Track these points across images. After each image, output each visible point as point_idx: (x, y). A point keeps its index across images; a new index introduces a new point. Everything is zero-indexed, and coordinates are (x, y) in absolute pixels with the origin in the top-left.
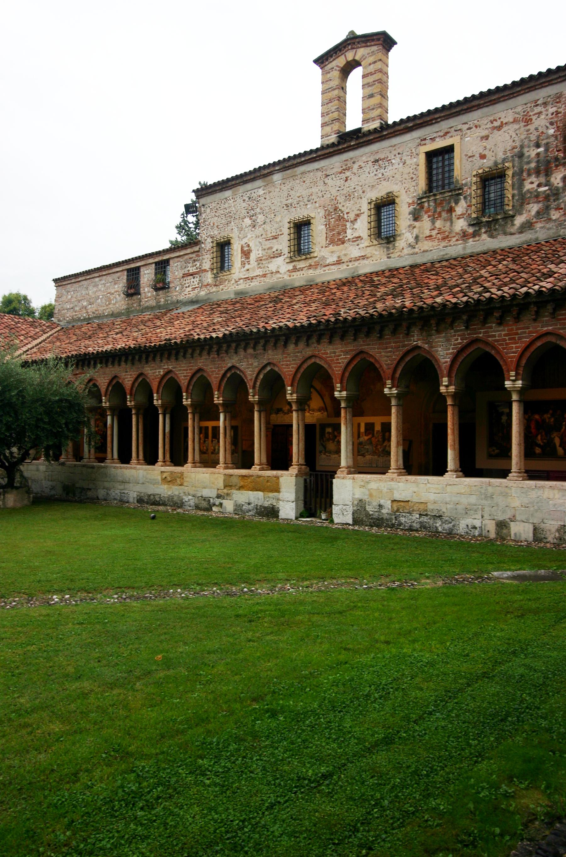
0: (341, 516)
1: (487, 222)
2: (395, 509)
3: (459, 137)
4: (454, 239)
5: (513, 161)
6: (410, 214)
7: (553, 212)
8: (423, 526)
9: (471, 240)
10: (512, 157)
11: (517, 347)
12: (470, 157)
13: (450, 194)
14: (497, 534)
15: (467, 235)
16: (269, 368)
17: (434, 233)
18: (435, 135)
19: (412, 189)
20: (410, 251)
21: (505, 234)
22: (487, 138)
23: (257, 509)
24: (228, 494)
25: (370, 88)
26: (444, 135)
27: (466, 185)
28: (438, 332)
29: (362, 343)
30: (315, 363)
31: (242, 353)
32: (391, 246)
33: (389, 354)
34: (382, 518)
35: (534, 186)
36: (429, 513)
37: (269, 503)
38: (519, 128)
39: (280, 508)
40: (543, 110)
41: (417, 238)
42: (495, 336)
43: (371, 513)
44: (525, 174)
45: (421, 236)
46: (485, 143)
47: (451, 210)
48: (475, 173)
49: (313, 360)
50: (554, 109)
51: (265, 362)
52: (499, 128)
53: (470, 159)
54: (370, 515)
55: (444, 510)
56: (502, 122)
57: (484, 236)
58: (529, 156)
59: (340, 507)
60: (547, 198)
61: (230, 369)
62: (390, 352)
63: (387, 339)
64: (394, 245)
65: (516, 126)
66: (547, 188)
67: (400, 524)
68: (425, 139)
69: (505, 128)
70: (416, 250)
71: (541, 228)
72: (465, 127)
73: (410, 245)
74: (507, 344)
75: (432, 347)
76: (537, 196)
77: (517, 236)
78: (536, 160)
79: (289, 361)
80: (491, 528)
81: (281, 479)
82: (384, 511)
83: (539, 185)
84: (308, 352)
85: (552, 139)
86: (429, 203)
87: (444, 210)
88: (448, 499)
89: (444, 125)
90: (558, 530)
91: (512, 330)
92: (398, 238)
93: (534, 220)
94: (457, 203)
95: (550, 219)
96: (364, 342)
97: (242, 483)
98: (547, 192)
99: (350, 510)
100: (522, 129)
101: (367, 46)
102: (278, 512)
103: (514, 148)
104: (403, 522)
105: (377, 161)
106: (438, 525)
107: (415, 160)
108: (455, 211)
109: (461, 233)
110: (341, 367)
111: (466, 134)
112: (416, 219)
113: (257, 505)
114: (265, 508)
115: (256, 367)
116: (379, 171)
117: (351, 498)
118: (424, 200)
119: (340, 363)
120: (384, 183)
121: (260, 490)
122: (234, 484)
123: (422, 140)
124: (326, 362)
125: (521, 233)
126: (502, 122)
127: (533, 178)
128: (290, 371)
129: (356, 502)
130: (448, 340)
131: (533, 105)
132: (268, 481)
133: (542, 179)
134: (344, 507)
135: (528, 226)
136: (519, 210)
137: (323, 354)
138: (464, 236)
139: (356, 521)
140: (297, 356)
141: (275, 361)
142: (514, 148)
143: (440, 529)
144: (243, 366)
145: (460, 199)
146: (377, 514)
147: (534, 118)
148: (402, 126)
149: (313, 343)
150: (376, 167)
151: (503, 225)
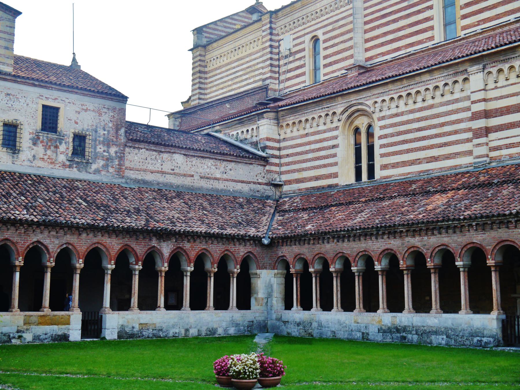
0: (111, 335)
1: (77, 161)
2: (141, 328)
3: (64, 105)
4: (58, 165)
5: (92, 133)
6: (30, 139)
7: (110, 168)
8: (154, 335)
9: (68, 169)
10: (92, 130)
11: (194, 253)
12: (69, 120)
13: (57, 137)
14: (185, 334)
15: (65, 166)
16: (65, 246)
17: (46, 157)
18: (49, 96)
19: (32, 124)
20: (29, 163)
21: (86, 171)
22: (79, 113)
23: (52, 337)
24: (27, 330)
25: (6, 43)
26: (54, 99)
27: (66, 135)
28: (164, 241)
29: (127, 240)
30: (97, 247)
31: (46, 233)
32: (15, 156)
33: (141, 248)
34: (134, 334)
35: (102, 150)
36: (157, 328)
37: (62, 332)
38: (96, 116)
39: (70, 335)
40: (107, 112)
41: (34, 156)
42: (186, 247)
43: (128, 331)
44: (97, 142)
45: (37, 156)
46: (77, 115)
47: (56, 147)
48: (73, 131)
49: (96, 245)
50: (112, 114)
51: (64, 242)
52: (86, 110)
53: (69, 121)
54: (127, 333)
55: (164, 326)
56: (87, 108)
57: (75, 169)
58: (100, 133)
59: (110, 330)
60: (107, 159)
61: (33, 243)
62: (141, 247)
63: (140, 240)
64: (18, 156)
65: (93, 114)
66: (107, 154)
67: (143, 336)
68: (42, 96)
69: (88, 112)
70: (33, 164)
71: (104, 175)
72: (67, 101)
73: (29, 160)
74: (190, 251)
75: (161, 248)
76: (103, 157)
77: (92, 175)
78: (103, 137)
79: (82, 244)
80: (183, 332)
81: (71, 316)
82: (135, 330)
83: (104, 151)
84: (95, 240)
85: (111, 129)
86: (43, 138)
87: (53, 146)
88: (165, 321)
89: (56, 94)
90: (206, 330)
91: (192, 245)
92: (21, 153)
93: (101, 169)
94: (61, 143)
95: (108, 171)
96: (128, 240)
97: (40, 321)
98: (108, 156)
99: (116, 331)
100: (97, 117)
101: (5, 13)
102: (69, 337)
103: (92, 125)
104: (144, 334)
105: (8, 94)
106: (161, 334)
107: (35, 106)
108: (59, 148)
109: (62, 163)
110: (115, 251)
111: (67, 105)
112: (35, 144)
113: (52, 334)
114: (59, 336)
115: (58, 244)
116: (9, 102)
117: (117, 324)
118: (40, 134)
119: (114, 249)
120: (13, 112)
121: (55, 324)
122: (33, 322)
123: (40, 95)
124: (105, 247)
125: (94, 174)
126: (87, 108)
127: (101, 146)
128: (83, 250)
129: (119, 327)
130: (168, 246)
131: (103, 106)
132: (62, 318)
133: (106, 149)
134: (113, 330)
135: (97, 171)
136: (94, 162)
137: (104, 243)
138: (63, 165)
139: (119, 337)
140: (87, 241)
141: (71, 242)
142: (92, 126)
143: (162, 336)
144: (46, 242)
145: (63, 142)
146: (131, 332)
147: (103, 114)
148: (31, 82)
149: (98, 236)
150: (7, 98)
151: (85, 166)
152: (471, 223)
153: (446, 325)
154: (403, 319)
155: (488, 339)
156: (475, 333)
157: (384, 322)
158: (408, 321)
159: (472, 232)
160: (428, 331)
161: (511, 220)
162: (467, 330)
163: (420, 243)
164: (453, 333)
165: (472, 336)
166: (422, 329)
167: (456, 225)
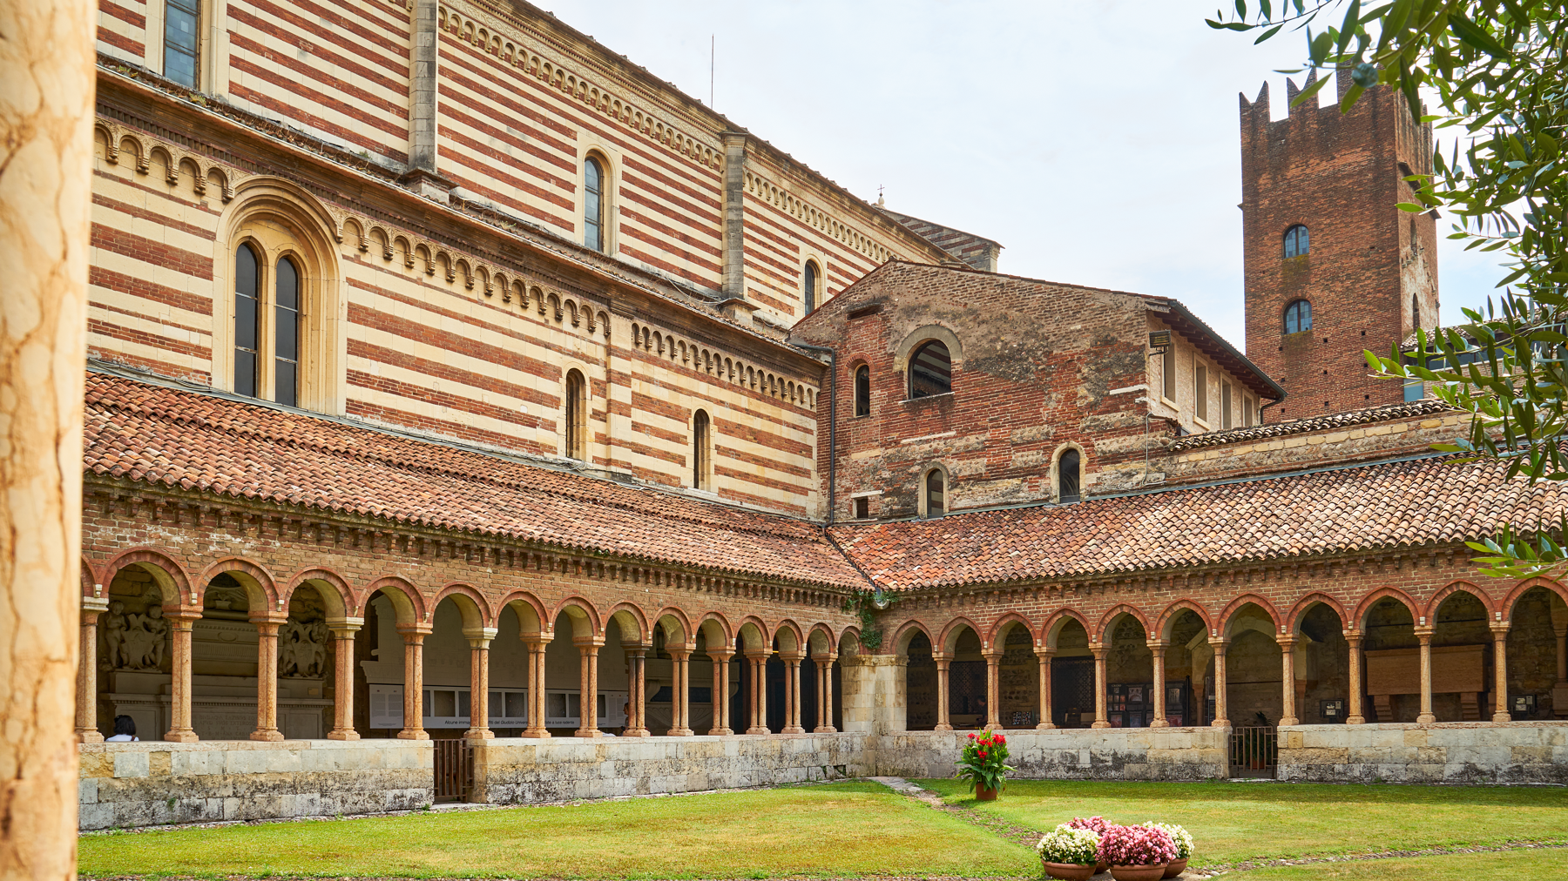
152: (406, 533)
153: (320, 767)
154: (194, 758)
155: (417, 790)
156: (392, 779)
157: (123, 769)
158: (211, 762)
159: (396, 554)
160: (270, 784)
161: (484, 545)
162: (371, 775)
163: (257, 554)
164: (337, 785)
165: (384, 787)
166: (254, 782)
167: (373, 529)
